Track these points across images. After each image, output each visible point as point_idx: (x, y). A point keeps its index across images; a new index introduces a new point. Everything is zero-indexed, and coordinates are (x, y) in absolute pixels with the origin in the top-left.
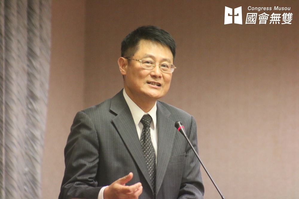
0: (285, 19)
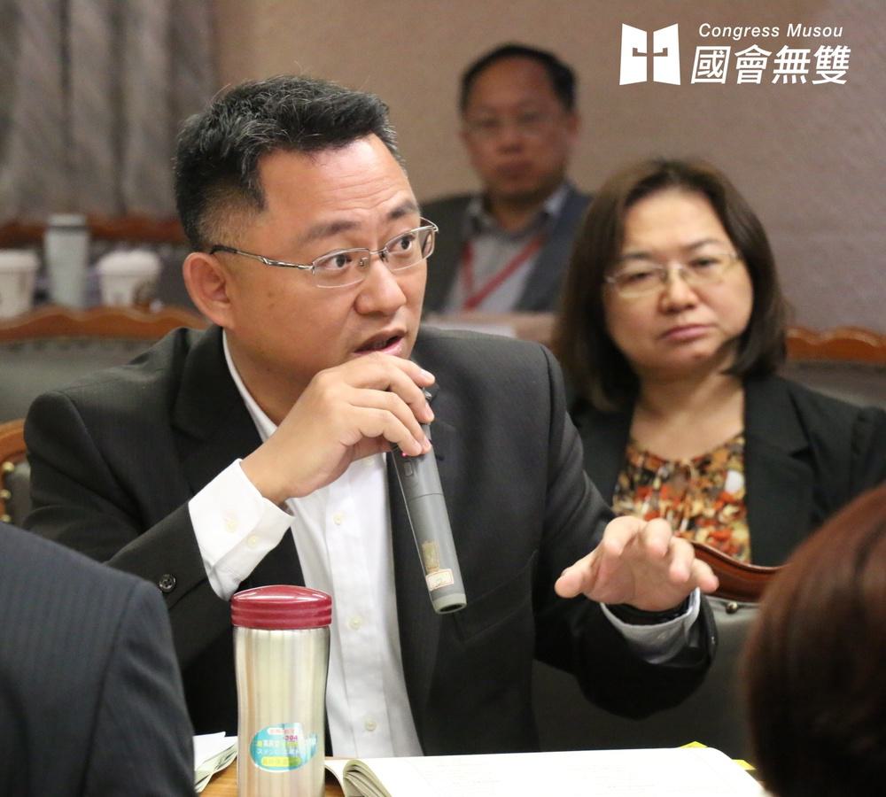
0: (825, 67)
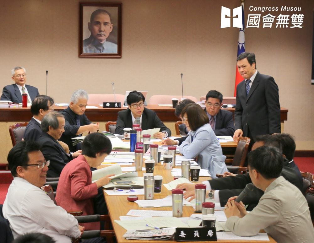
0: (295, 22)
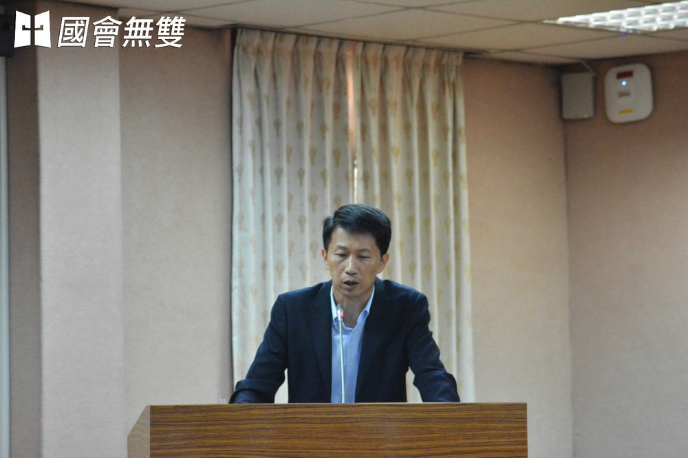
0: (165, 34)
